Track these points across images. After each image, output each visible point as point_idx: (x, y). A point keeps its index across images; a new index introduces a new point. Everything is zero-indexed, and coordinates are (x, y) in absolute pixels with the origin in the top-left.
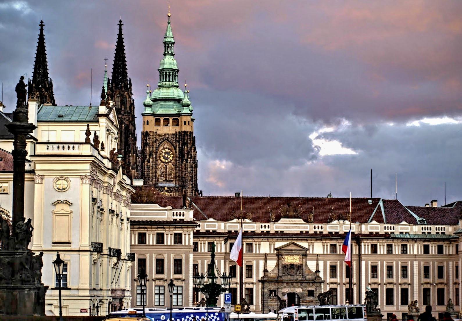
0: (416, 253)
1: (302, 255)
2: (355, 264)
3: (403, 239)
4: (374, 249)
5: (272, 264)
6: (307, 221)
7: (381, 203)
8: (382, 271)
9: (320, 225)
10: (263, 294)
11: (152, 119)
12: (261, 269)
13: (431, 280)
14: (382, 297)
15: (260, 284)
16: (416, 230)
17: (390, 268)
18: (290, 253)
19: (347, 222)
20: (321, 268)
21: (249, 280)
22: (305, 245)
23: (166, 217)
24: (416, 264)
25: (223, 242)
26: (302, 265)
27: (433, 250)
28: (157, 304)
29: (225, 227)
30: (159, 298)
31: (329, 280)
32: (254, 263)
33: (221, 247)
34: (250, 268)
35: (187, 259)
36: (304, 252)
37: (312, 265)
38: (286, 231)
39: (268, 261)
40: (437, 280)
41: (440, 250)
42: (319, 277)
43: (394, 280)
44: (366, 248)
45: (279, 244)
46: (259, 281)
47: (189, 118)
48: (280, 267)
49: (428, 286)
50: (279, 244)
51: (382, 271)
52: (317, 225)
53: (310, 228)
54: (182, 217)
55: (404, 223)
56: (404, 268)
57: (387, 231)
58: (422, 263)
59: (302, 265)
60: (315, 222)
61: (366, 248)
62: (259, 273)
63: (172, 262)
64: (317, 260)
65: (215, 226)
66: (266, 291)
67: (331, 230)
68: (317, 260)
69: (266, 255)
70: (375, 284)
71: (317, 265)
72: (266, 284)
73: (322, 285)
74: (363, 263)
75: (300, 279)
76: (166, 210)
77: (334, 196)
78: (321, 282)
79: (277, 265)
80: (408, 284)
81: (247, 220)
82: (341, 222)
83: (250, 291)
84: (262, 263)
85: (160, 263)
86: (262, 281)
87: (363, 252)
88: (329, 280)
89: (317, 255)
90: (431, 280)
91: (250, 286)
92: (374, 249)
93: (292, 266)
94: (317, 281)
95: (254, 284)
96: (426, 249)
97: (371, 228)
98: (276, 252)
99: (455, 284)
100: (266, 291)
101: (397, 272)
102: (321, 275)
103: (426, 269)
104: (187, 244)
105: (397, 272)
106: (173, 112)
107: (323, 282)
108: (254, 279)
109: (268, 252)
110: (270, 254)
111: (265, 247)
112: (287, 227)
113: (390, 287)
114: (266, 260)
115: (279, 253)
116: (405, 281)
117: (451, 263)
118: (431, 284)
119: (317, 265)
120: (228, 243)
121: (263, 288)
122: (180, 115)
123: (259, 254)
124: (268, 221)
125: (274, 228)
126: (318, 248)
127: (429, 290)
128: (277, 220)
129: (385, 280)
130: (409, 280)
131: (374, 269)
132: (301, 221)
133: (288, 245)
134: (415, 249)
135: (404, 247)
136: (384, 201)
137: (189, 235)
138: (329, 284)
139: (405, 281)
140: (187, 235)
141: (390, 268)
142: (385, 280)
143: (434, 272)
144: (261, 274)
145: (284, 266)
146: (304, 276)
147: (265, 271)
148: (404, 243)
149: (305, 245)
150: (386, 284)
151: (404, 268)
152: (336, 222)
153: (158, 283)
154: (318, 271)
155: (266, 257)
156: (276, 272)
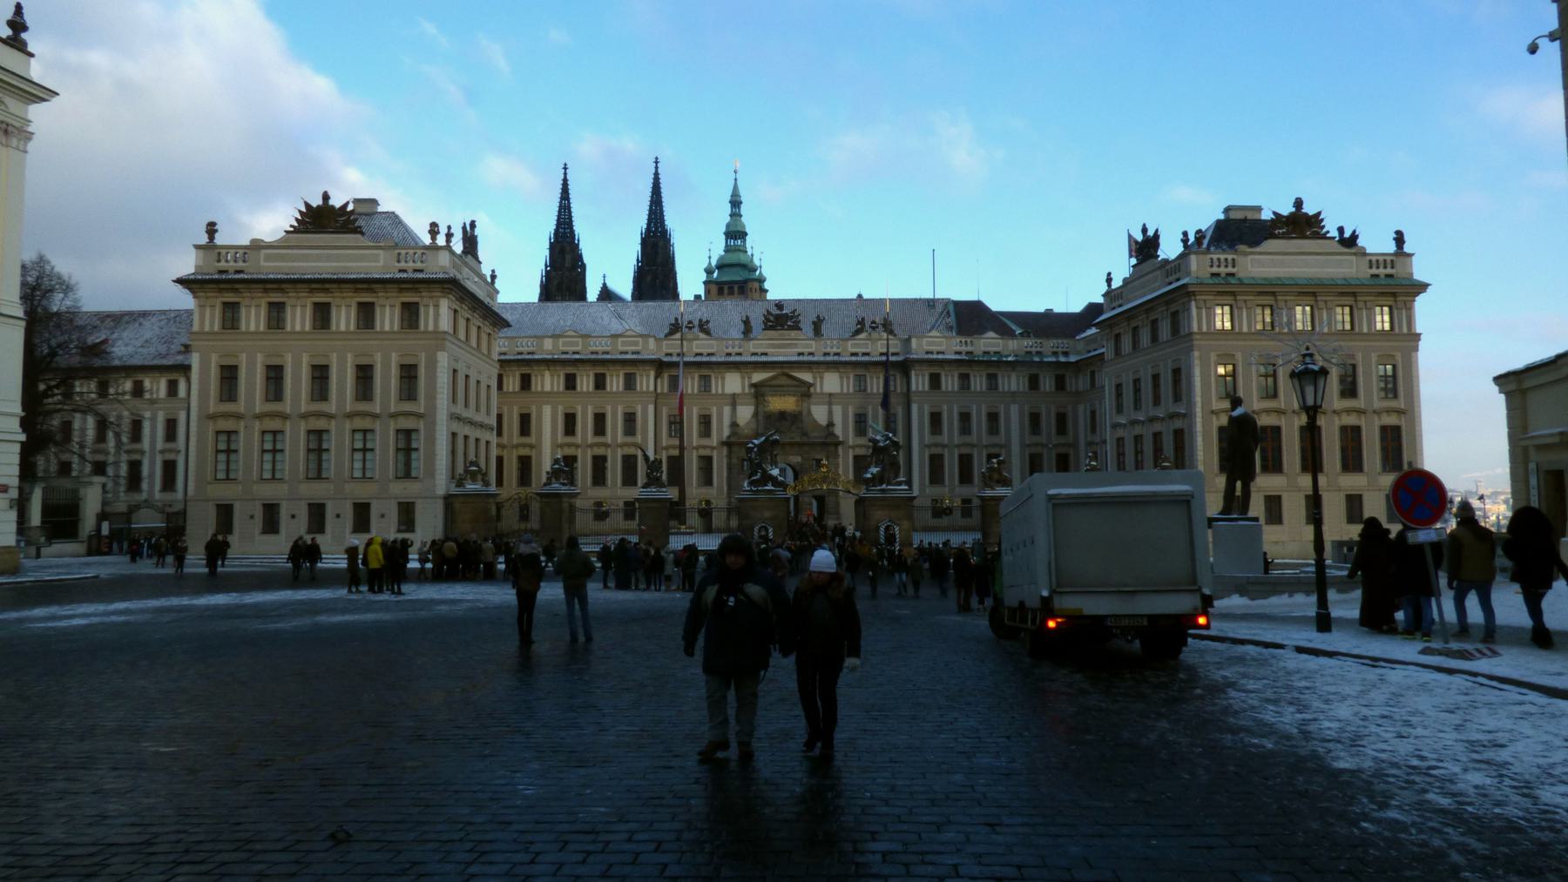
0: (1014, 387)
2: (899, 411)
3: (989, 363)
4: (935, 381)
5: (745, 413)
7: (951, 308)
8: (951, 422)
10: (730, 468)
11: (714, 288)
12: (727, 422)
13: (1043, 439)
14: (951, 468)
15: (725, 450)
16: (1012, 347)
17: (965, 417)
18: (779, 390)
19: (885, 335)
20: (838, 420)
21: (705, 442)
22: (806, 377)
23: (381, 263)
24: (1014, 409)
25: (652, 374)
26: (800, 413)
27: (1047, 383)
28: (358, 474)
30: (364, 460)
31: (852, 439)
32: (714, 411)
33: (647, 382)
34: (705, 421)
35: (432, 364)
36: (804, 389)
37: (819, 413)
39: (739, 408)
40: (1056, 440)
41: (1060, 383)
42: (832, 434)
43: (973, 439)
44: (919, 382)
45: (758, 377)
46: (724, 443)
47: (756, 285)
48: (761, 418)
49: (1039, 450)
50: (758, 377)
51: (951, 422)
54: (419, 265)
55: (991, 334)
56: (993, 417)
58: (1026, 408)
59: (800, 413)
61: (919, 382)
62: (721, 430)
63: (394, 371)
64: (830, 404)
65: (636, 344)
66: (735, 461)
68: (830, 404)
69: (734, 396)
70: (936, 445)
71: (830, 412)
72: (735, 449)
73: (840, 449)
74: (915, 408)
75: (798, 439)
76: (380, 248)
77: (865, 297)
78: (837, 444)
79: (756, 414)
80: (1001, 446)
81: (702, 335)
82: (875, 335)
83: (706, 463)
84: (727, 410)
85: (364, 374)
86: (728, 444)
87: (914, 388)
88: (851, 440)
89: (830, 395)
90: (1043, 439)
91: (707, 452)
92: (935, 381)
93: (782, 415)
94: (829, 442)
95: (712, 448)
96: (1034, 382)
99: (1089, 444)
100: (735, 461)
101: (979, 422)
102: (838, 431)
103: (1035, 419)
104: (431, 328)
105: (979, 422)
106: (738, 278)
107: (841, 443)
108: (714, 441)
109: (738, 390)
110: (743, 394)
111: (733, 383)
112: (773, 346)
113: (965, 451)
114: (734, 405)
115: (759, 392)
116: (995, 440)
117: (1081, 408)
118: (1043, 445)
119: (830, 412)
120: (666, 376)
121: (729, 456)
122: (746, 282)
123: (723, 395)
126: (831, 383)
127: (1040, 455)
129: (957, 439)
130: (1002, 439)
131: (936, 419)
133: (773, 378)
134: (1013, 382)
135: (992, 378)
136: (957, 304)
137: (437, 306)
138: (853, 447)
139: (995, 440)
140: (431, 310)
141: (965, 417)
142: (957, 439)
143: (1048, 423)
144: (726, 432)
145: (769, 417)
146: (805, 434)
147: (734, 425)
148: (992, 371)
149: (806, 377)
150: (958, 446)
151: (993, 417)
152: (863, 336)
153: (360, 423)
154: (831, 424)
155: (734, 400)
156: (753, 426)
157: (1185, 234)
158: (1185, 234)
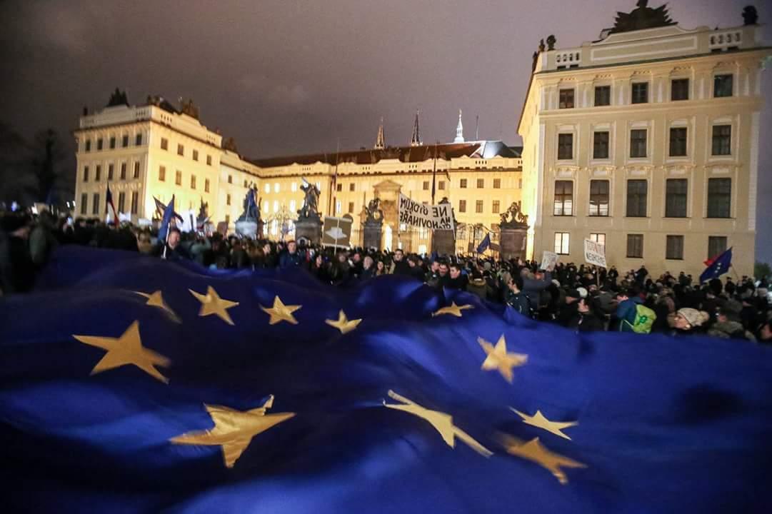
1: (396, 192)
6: (402, 160)
9: (415, 164)
18: (385, 190)
29: (330, 169)
38: (384, 171)
50: (378, 180)
52: (412, 164)
53: (405, 167)
57: (478, 165)
60: (410, 161)
67: (424, 169)
97: (461, 163)
98: (374, 189)
115: (377, 189)
121: (361, 219)
124: (369, 163)
125: (373, 168)
128: (377, 161)
132: (398, 161)
144: (361, 209)
149: (398, 180)
157: (542, 41)
158: (542, 41)
